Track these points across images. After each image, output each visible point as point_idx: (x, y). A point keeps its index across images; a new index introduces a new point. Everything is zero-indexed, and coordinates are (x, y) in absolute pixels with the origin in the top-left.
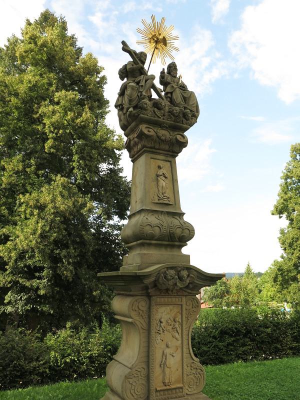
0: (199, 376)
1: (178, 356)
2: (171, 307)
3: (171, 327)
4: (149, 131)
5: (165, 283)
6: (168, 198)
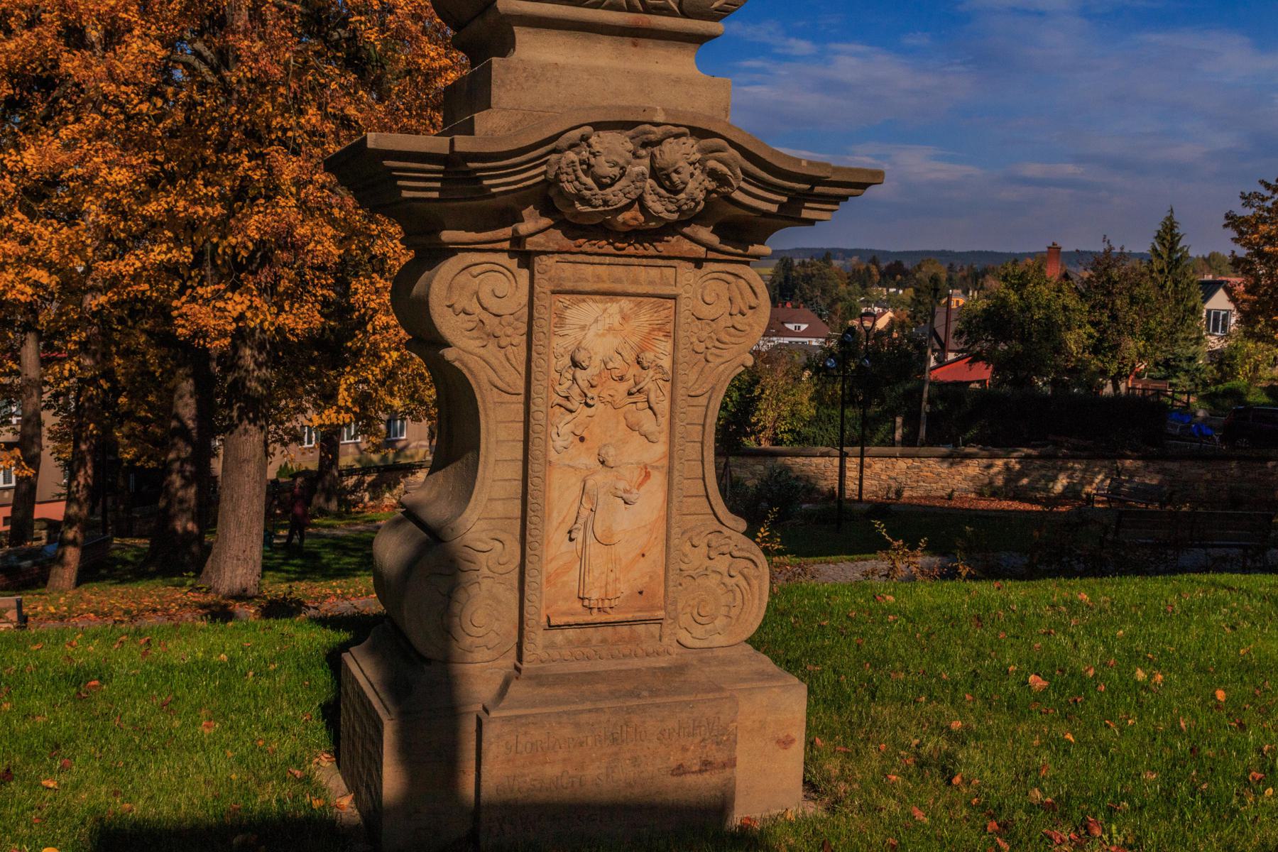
0: (743, 583)
1: (651, 500)
2: (625, 303)
3: (623, 387)
5: (587, 193)
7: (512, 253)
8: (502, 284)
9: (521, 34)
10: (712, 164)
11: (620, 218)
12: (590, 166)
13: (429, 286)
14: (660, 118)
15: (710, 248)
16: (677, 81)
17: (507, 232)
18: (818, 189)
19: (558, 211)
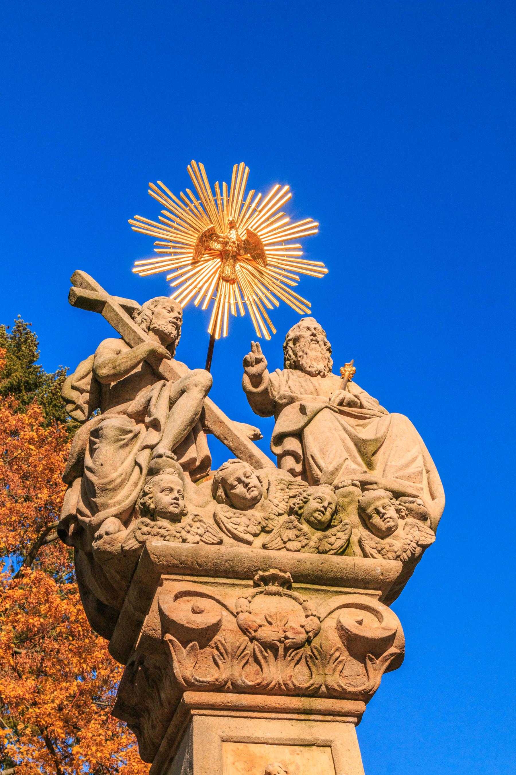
4: (195, 611)
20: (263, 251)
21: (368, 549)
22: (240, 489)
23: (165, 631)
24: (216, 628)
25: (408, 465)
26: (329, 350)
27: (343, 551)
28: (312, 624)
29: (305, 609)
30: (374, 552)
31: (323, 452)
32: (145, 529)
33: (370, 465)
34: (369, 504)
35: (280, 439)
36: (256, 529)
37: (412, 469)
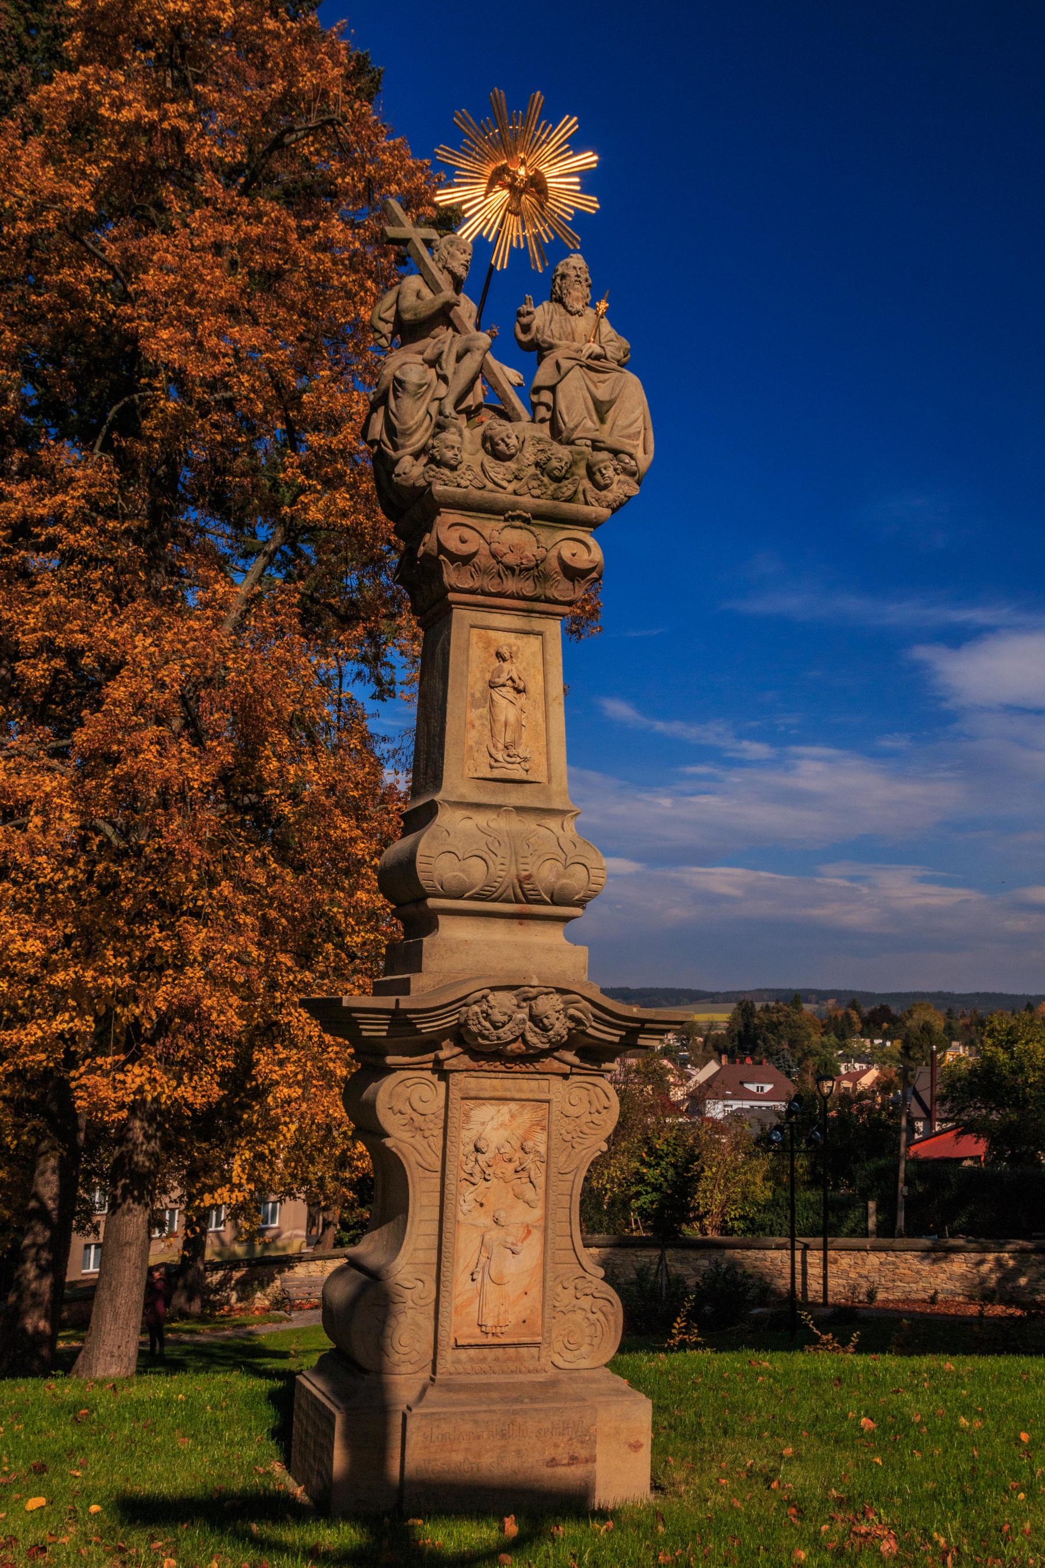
0: (602, 1318)
1: (531, 1252)
2: (513, 1106)
3: (511, 1167)
6: (525, 760)
7: (434, 1071)
8: (426, 1092)
9: (442, 919)
10: (571, 1011)
11: (509, 1048)
12: (488, 1015)
13: (376, 1094)
14: (535, 983)
15: (572, 1066)
16: (550, 950)
17: (431, 1056)
18: (647, 1026)
19: (465, 1042)
20: (546, 188)
21: (589, 498)
22: (502, 447)
23: (439, 553)
24: (474, 554)
25: (630, 425)
26: (589, 286)
27: (570, 500)
28: (540, 553)
29: (538, 541)
30: (593, 501)
31: (568, 408)
32: (432, 473)
33: (602, 421)
34: (595, 465)
35: (537, 390)
36: (510, 477)
37: (633, 430)
